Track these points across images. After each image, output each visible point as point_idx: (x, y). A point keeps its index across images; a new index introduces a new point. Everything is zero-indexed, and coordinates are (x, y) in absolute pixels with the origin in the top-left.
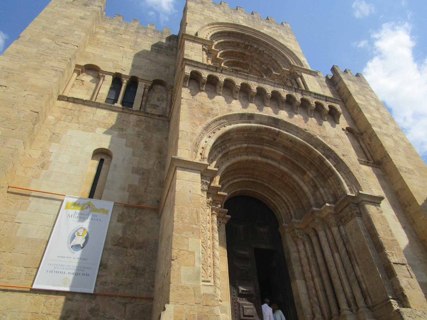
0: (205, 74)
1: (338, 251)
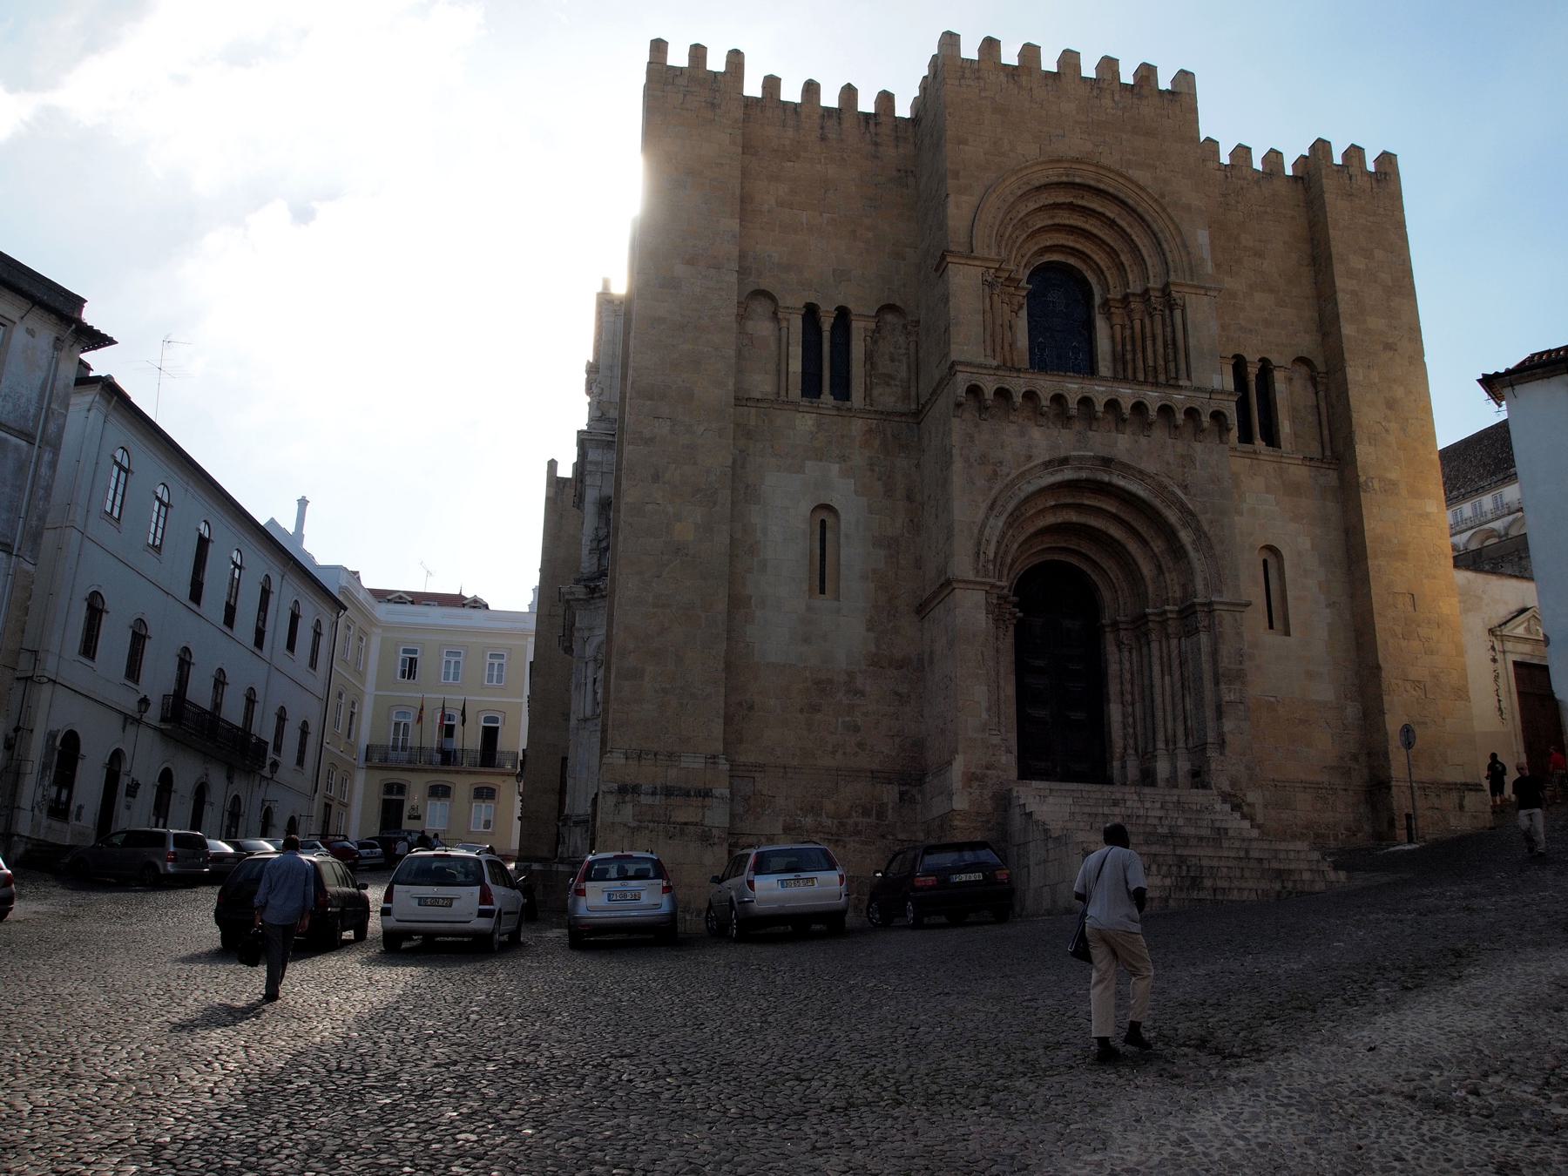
0: (989, 386)
1: (1170, 674)
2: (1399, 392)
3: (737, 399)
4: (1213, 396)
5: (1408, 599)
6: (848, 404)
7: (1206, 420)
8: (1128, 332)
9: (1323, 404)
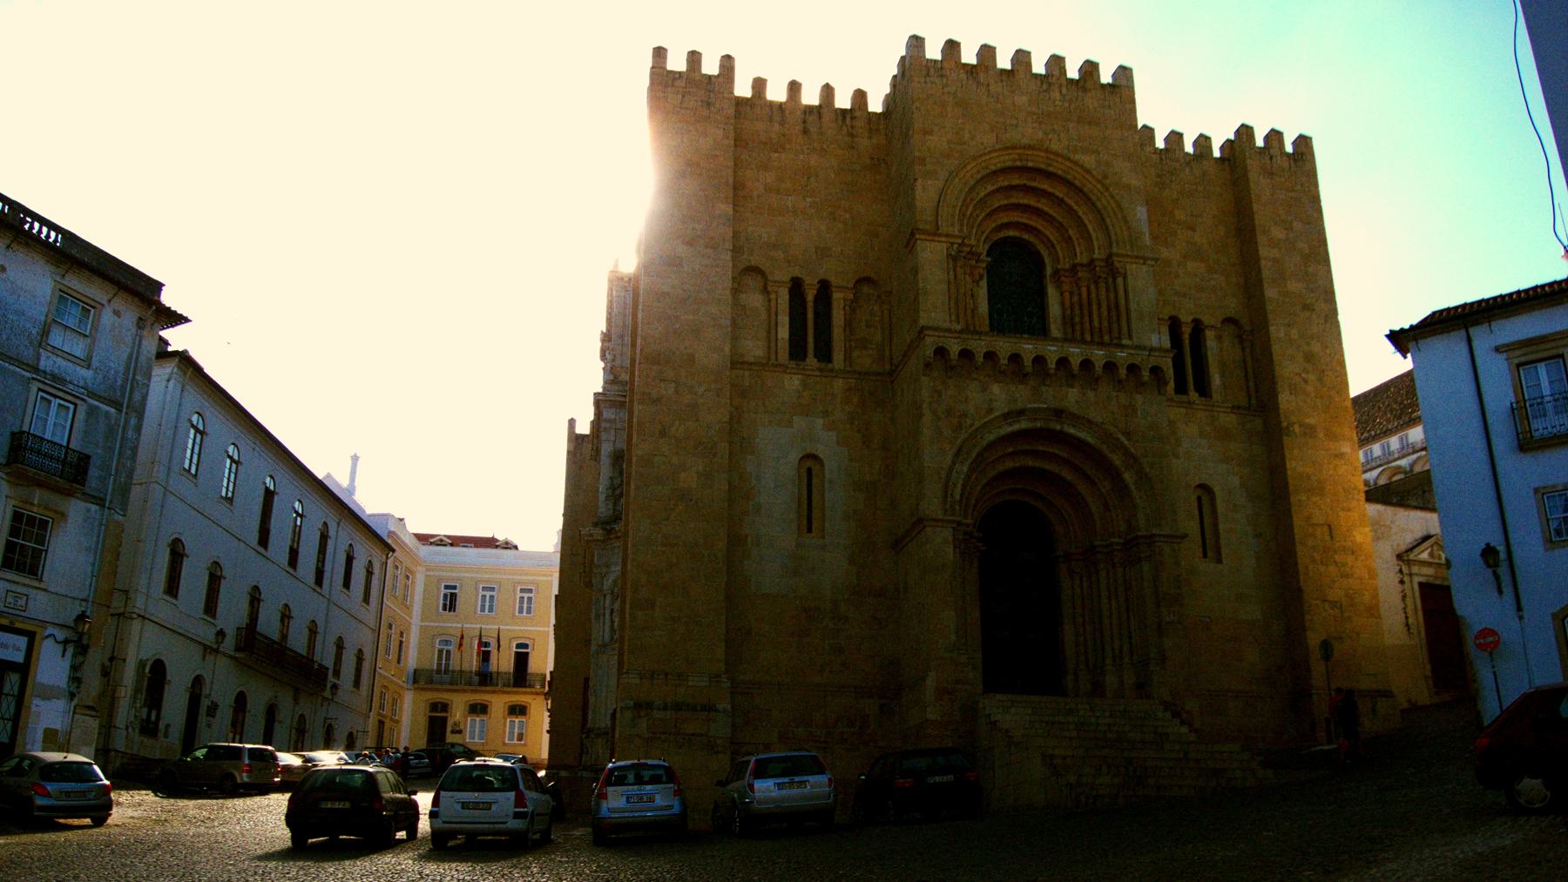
0: (954, 348)
2: (1316, 348)
3: (732, 363)
4: (1152, 353)
5: (1325, 529)
6: (830, 366)
7: (1146, 375)
8: (1075, 299)
9: (1249, 359)
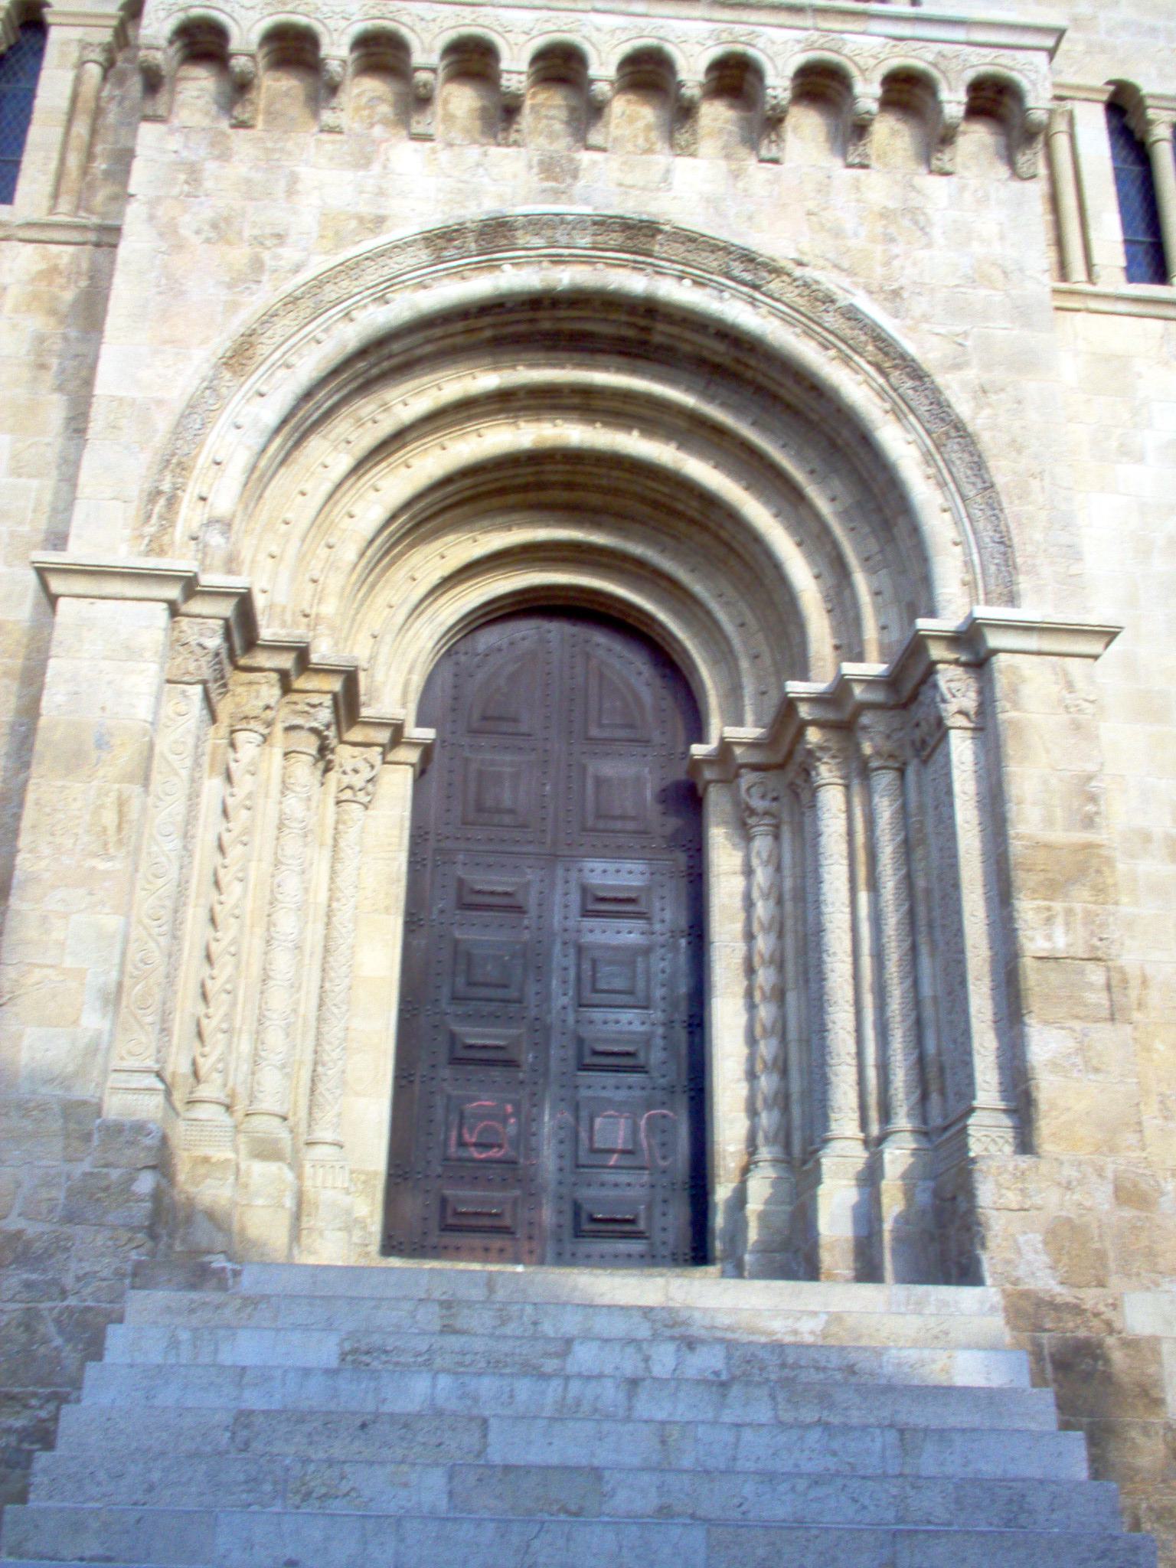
1: (874, 886)
